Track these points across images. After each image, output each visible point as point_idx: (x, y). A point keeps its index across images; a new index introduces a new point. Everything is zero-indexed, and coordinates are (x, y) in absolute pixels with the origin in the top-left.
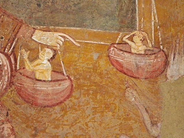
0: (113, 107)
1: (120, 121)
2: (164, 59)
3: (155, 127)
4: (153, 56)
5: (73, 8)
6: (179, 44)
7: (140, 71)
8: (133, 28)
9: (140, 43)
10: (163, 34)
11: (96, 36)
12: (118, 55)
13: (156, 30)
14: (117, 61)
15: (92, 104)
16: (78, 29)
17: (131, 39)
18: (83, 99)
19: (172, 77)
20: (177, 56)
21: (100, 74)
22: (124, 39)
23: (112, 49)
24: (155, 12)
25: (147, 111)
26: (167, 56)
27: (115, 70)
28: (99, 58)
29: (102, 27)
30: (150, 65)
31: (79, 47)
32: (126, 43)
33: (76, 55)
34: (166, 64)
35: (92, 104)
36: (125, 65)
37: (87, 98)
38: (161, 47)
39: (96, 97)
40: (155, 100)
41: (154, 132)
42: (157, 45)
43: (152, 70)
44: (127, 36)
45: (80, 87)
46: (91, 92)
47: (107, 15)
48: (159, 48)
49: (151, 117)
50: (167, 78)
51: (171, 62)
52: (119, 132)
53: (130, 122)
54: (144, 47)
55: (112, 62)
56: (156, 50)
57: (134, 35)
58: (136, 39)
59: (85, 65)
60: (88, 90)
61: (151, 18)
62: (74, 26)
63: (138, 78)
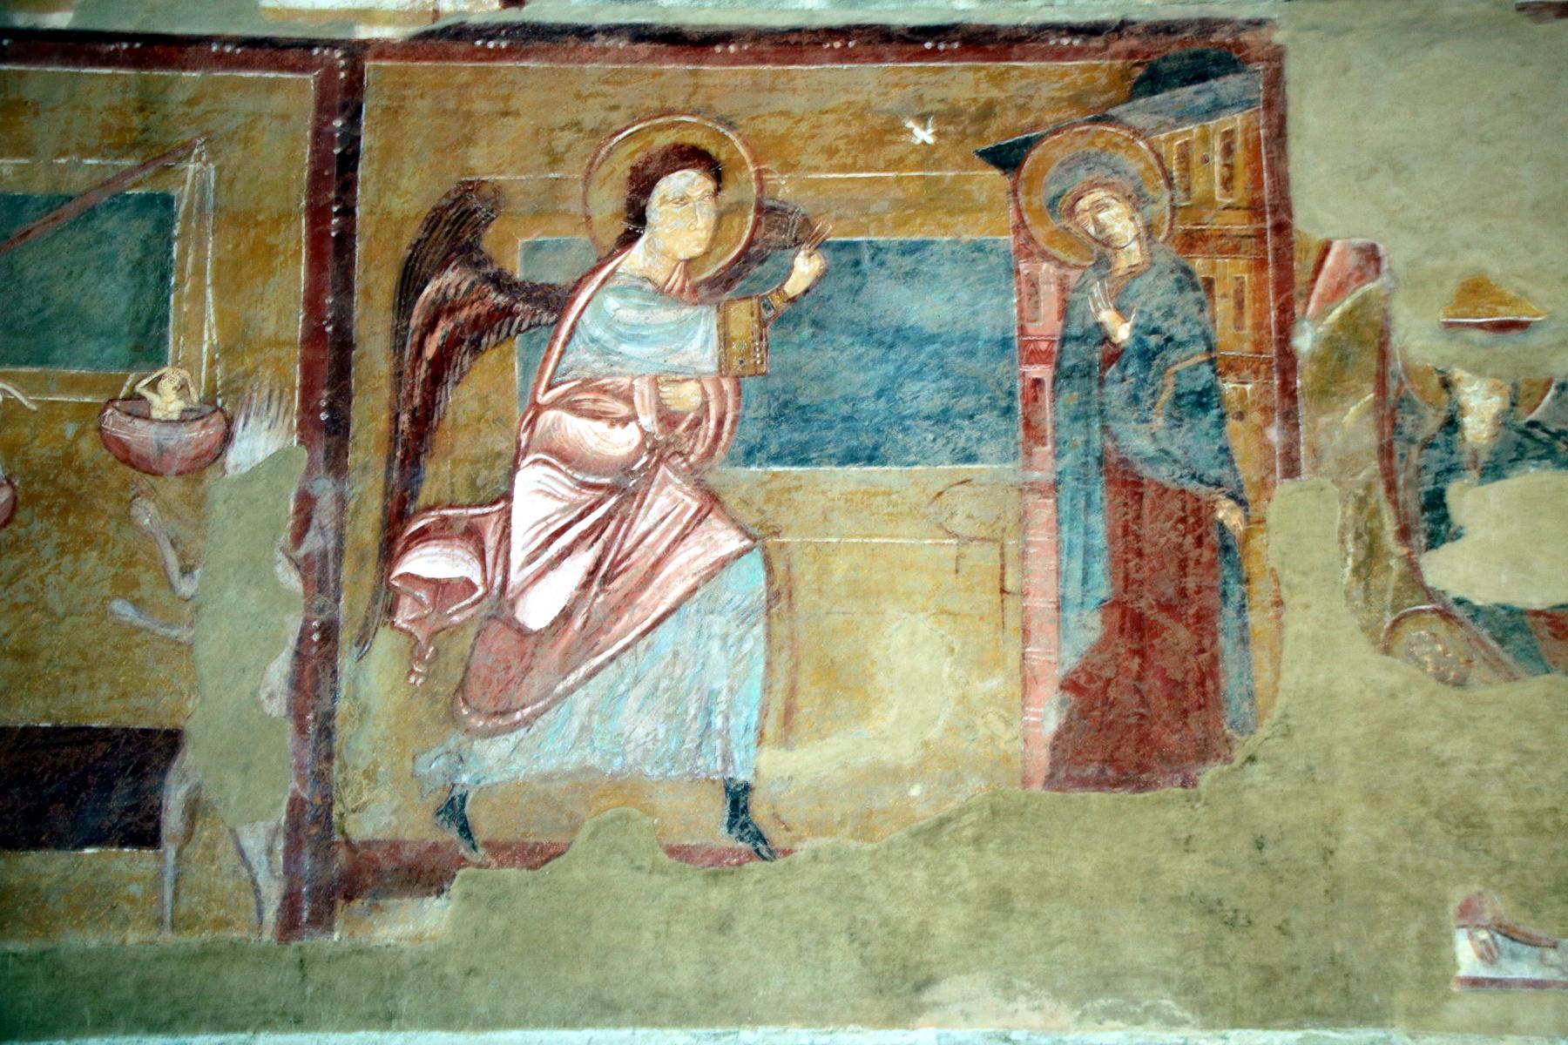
0: (100, 539)
1: (113, 571)
2: (222, 427)
3: (187, 579)
4: (199, 424)
5: (26, 323)
6: (259, 391)
7: (167, 458)
8: (160, 361)
9: (172, 396)
10: (228, 371)
11: (74, 384)
12: (122, 425)
13: (212, 363)
14: (118, 440)
15: (56, 536)
16: (35, 370)
17: (153, 386)
18: (38, 526)
19: (236, 466)
20: (252, 421)
21: (80, 471)
22: (139, 388)
23: (109, 411)
24: (213, 319)
25: (173, 545)
26: (229, 422)
27: (111, 459)
28: (80, 433)
29: (90, 363)
30: (188, 443)
31: (35, 412)
32: (141, 398)
33: (27, 430)
34: (227, 438)
35: (56, 536)
36: (135, 448)
37: (45, 524)
38: (219, 402)
39: (66, 520)
40: (194, 520)
41: (186, 587)
42: (210, 399)
43: (193, 453)
44: (145, 382)
45: (32, 499)
46: (56, 510)
47: (102, 334)
48: (214, 402)
49: (182, 557)
50: (225, 472)
51: (239, 434)
52: (109, 593)
53: (134, 571)
54: (180, 405)
55: (108, 441)
56: (209, 409)
57: (160, 378)
58: (167, 386)
59: (46, 451)
60: (50, 507)
61: (201, 336)
62: (26, 363)
63: (161, 475)
